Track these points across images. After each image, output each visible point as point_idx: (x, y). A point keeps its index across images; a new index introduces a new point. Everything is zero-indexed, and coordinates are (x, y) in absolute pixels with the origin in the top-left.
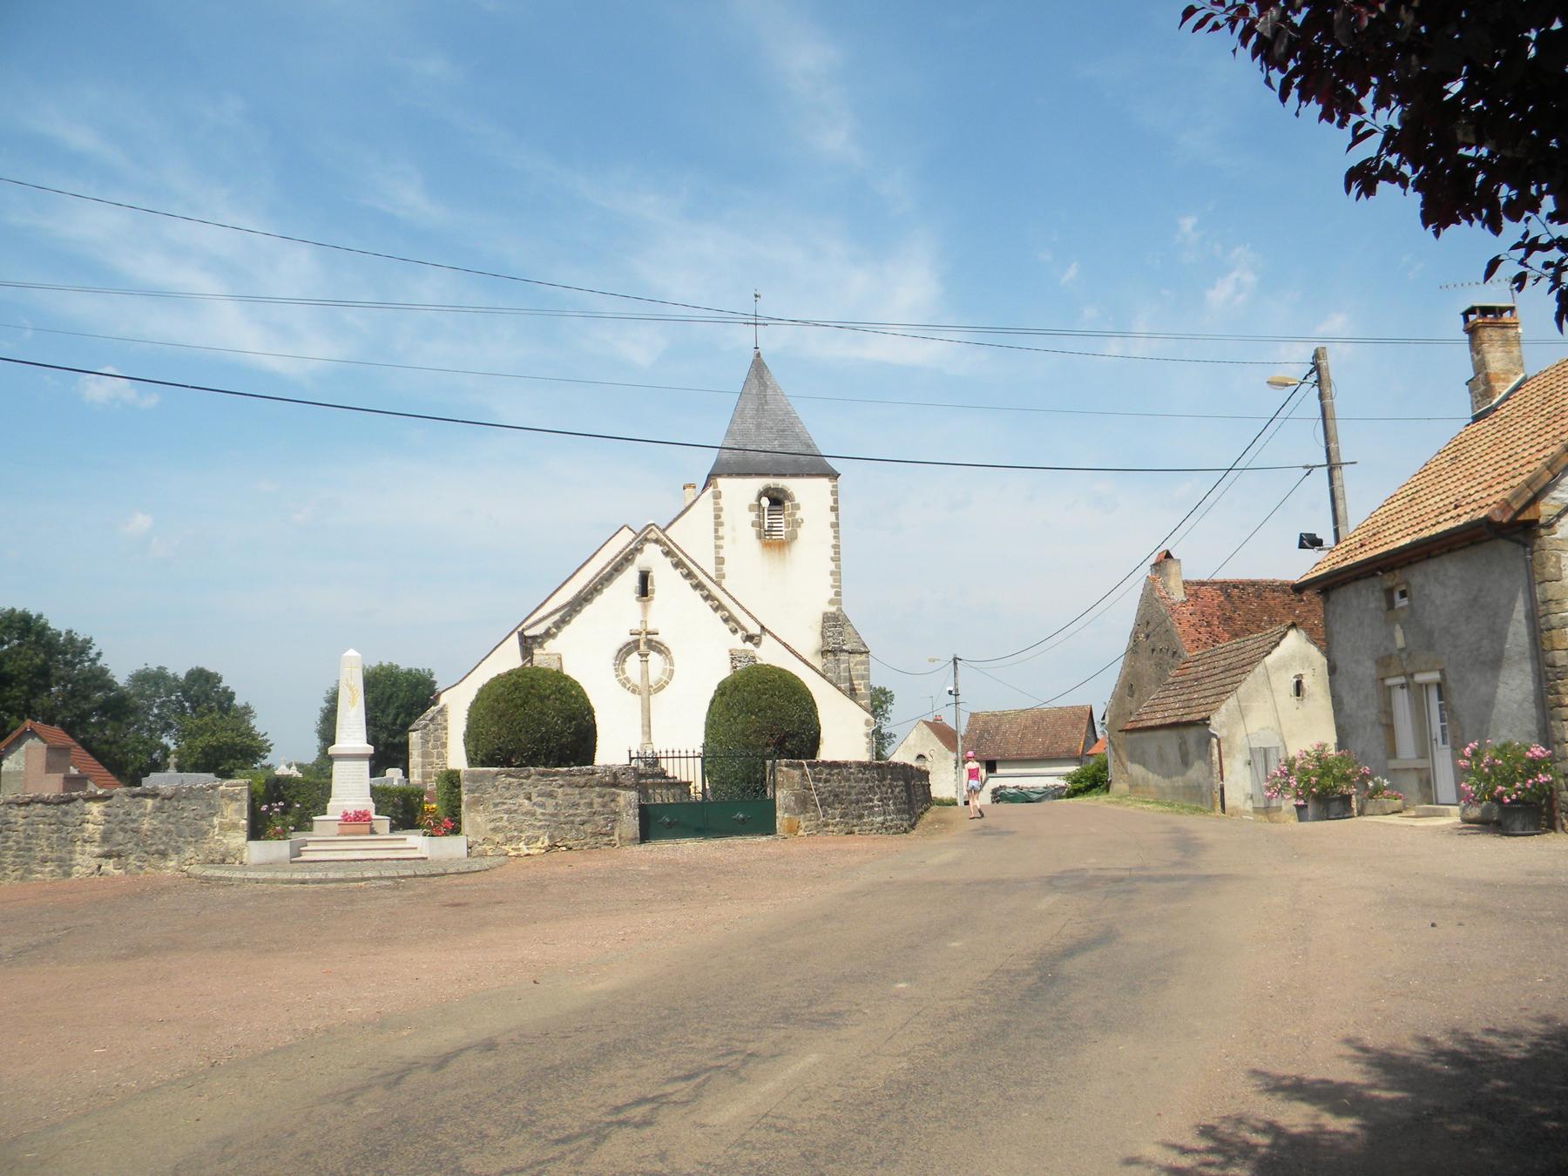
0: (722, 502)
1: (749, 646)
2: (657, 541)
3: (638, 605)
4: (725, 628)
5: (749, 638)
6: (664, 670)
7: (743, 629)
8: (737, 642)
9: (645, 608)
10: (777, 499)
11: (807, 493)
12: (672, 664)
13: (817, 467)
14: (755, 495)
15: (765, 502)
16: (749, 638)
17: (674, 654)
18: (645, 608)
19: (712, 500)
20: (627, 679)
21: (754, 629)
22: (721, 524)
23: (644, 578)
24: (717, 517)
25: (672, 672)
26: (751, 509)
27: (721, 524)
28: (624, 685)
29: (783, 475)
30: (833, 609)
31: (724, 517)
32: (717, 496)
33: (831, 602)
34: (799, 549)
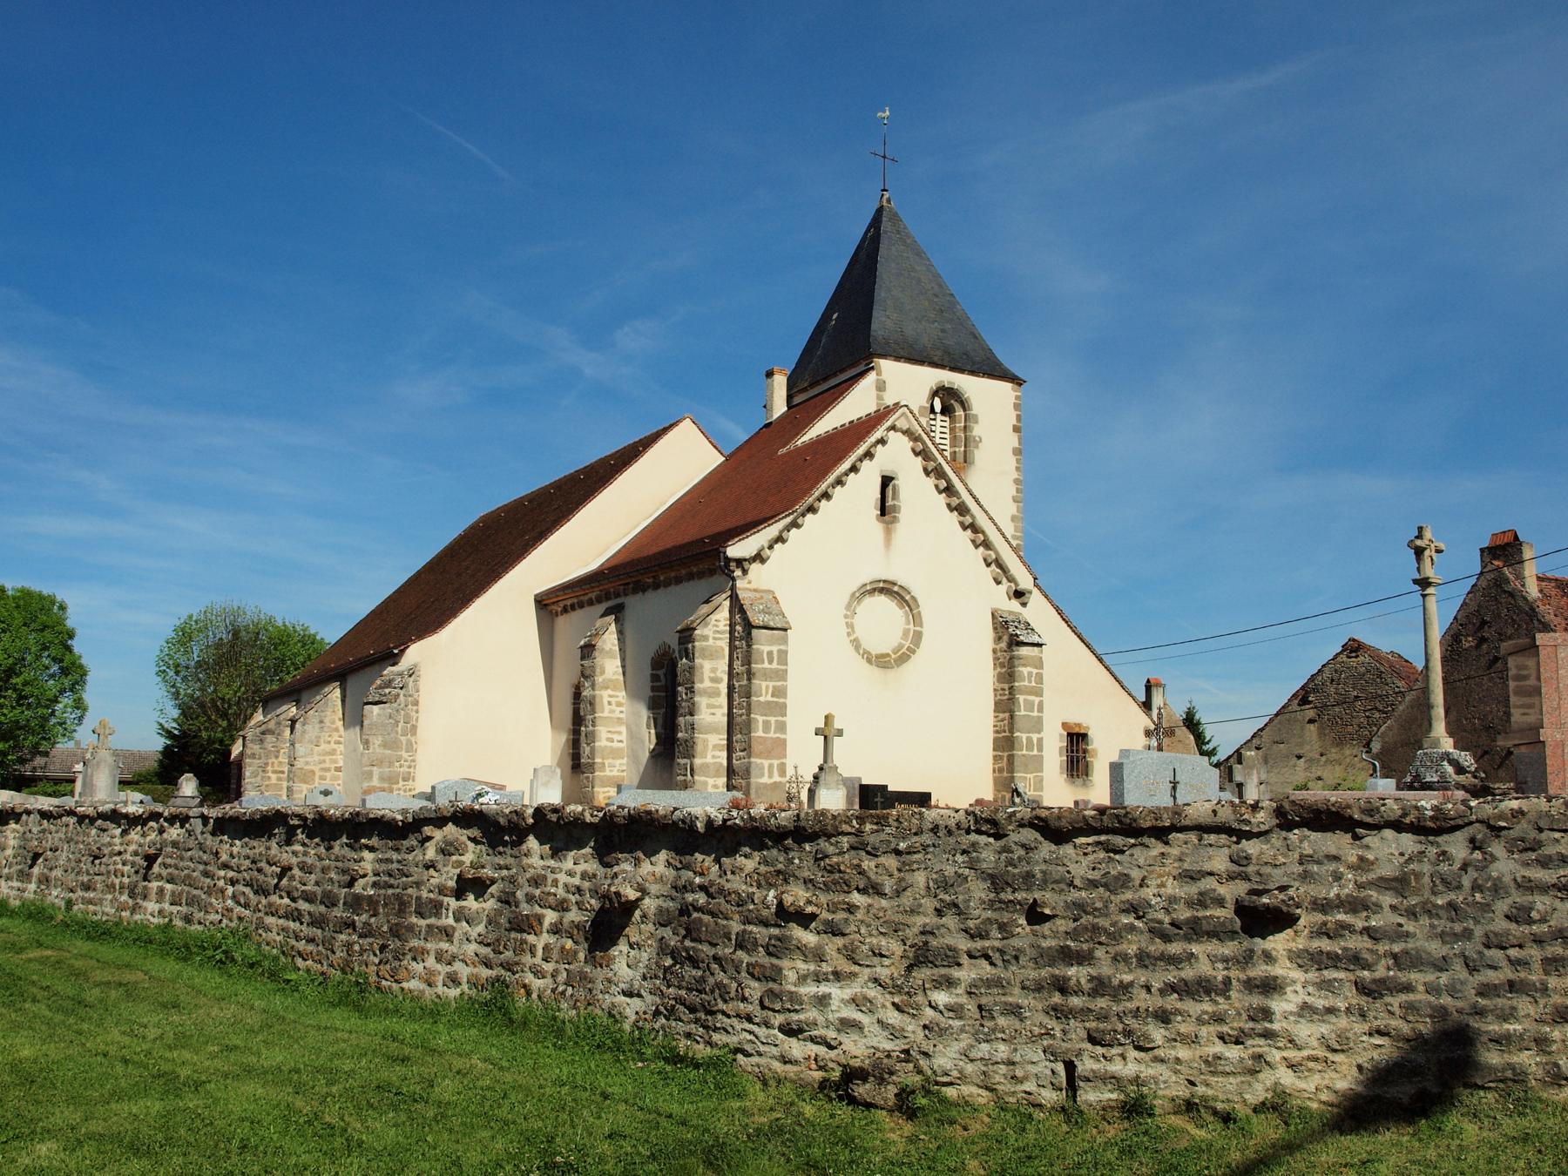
1: (1014, 605)
2: (905, 432)
4: (987, 573)
5: (1019, 594)
6: (906, 633)
7: (1011, 579)
9: (888, 533)
10: (949, 400)
11: (990, 400)
12: (917, 619)
13: (993, 369)
14: (926, 394)
16: (1019, 594)
18: (888, 533)
19: (874, 392)
23: (886, 481)
25: (918, 637)
29: (961, 370)
32: (881, 386)
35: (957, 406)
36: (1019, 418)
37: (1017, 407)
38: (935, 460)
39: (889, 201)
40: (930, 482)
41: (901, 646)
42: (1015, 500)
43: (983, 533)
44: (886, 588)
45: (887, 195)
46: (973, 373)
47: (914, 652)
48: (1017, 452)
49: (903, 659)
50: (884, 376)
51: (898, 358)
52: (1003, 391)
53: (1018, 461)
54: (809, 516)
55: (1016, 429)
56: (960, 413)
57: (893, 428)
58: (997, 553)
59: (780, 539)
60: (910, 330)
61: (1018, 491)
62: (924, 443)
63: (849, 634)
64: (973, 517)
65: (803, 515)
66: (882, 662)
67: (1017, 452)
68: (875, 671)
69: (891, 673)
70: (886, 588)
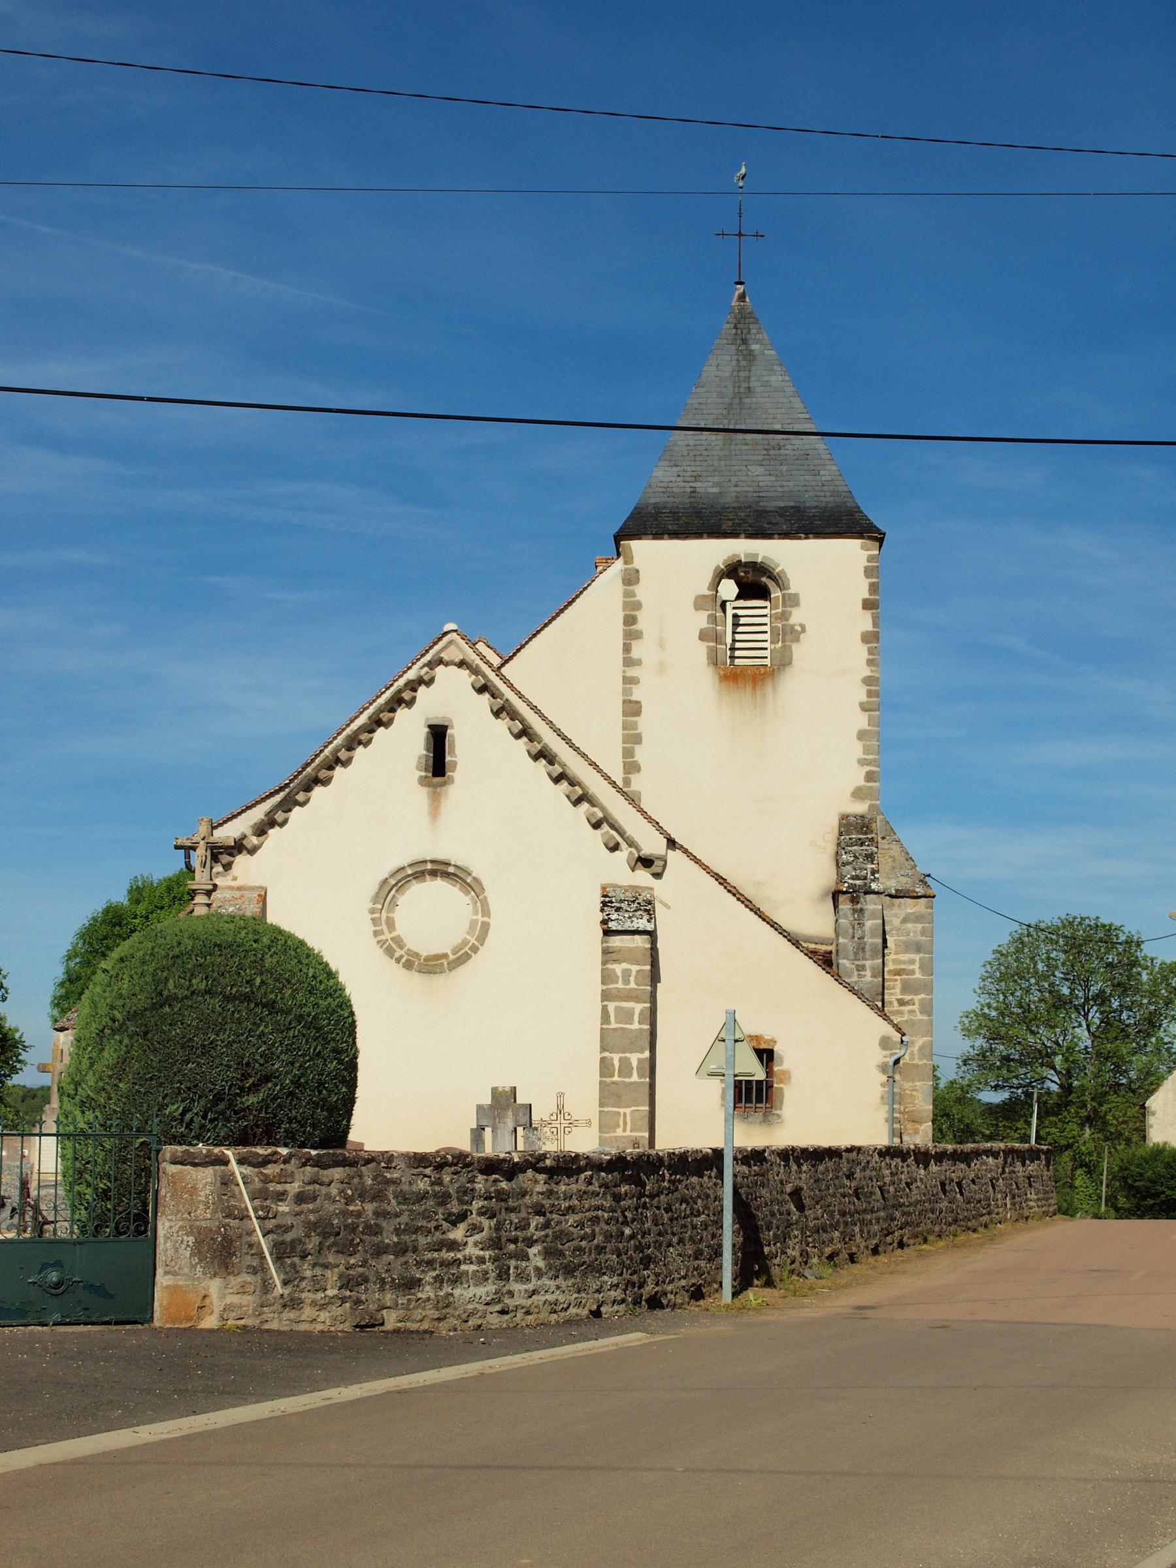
0: (641, 592)
1: (643, 877)
2: (462, 664)
3: (421, 795)
5: (646, 862)
6: (473, 923)
7: (631, 843)
8: (617, 870)
9: (435, 800)
10: (754, 582)
11: (824, 575)
14: (708, 576)
15: (729, 589)
16: (646, 862)
17: (492, 894)
18: (435, 800)
19: (618, 588)
20: (398, 941)
21: (653, 845)
22: (638, 635)
23: (438, 736)
24: (630, 620)
25: (485, 927)
26: (699, 603)
27: (638, 635)
28: (389, 952)
30: (861, 808)
31: (644, 622)
32: (631, 579)
33: (858, 794)
34: (793, 688)
35: (771, 585)
36: (873, 588)
37: (868, 572)
38: (501, 695)
39: (742, 297)
40: (502, 726)
41: (465, 943)
42: (864, 707)
43: (579, 784)
44: (439, 870)
45: (741, 288)
46: (786, 535)
47: (475, 949)
48: (868, 638)
49: (462, 957)
50: (637, 563)
51: (658, 536)
52: (847, 555)
53: (870, 651)
54: (318, 791)
55: (867, 605)
56: (776, 593)
57: (441, 662)
58: (603, 809)
59: (272, 823)
60: (708, 487)
61: (870, 694)
62: (484, 676)
63: (376, 934)
64: (563, 765)
65: (308, 789)
66: (431, 966)
67: (868, 638)
68: (414, 978)
69: (438, 981)
70: (439, 870)
